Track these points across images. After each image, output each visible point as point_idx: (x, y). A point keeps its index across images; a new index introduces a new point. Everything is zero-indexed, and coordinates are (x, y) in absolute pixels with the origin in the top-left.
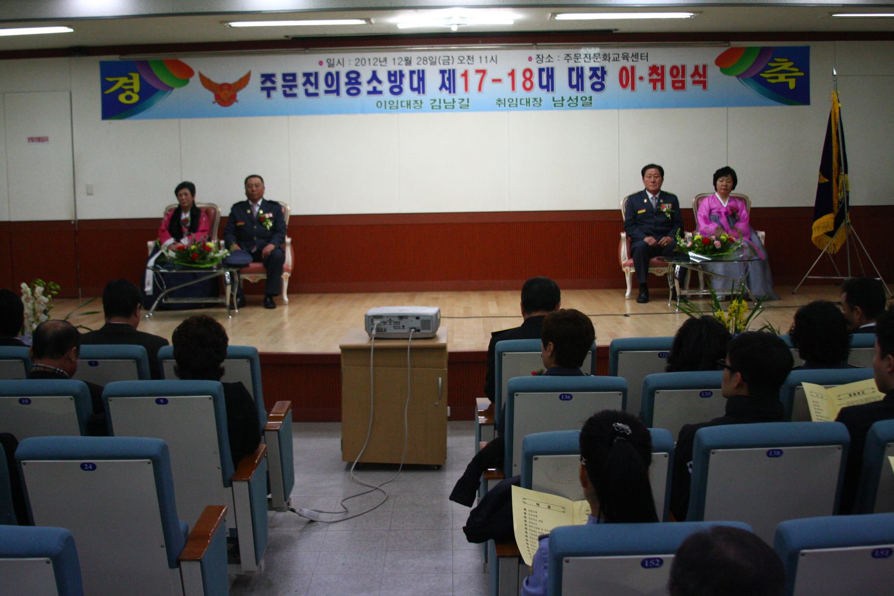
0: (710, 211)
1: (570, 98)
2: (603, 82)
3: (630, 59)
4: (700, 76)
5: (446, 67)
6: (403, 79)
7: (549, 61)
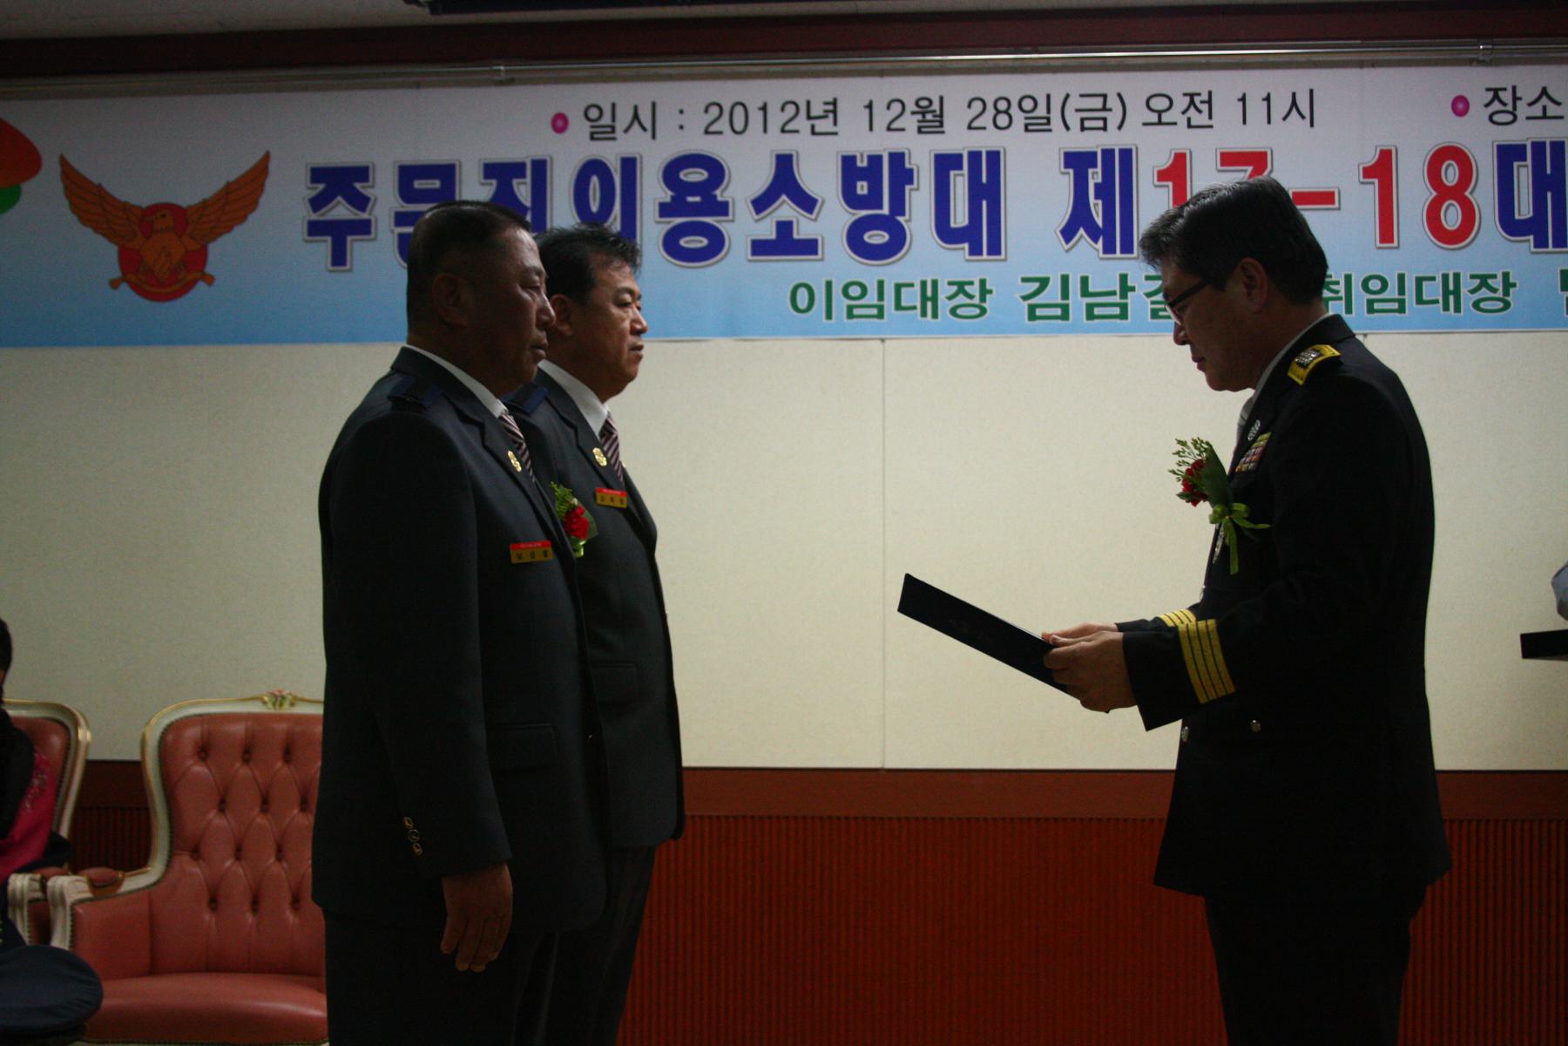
7: (1545, 116)
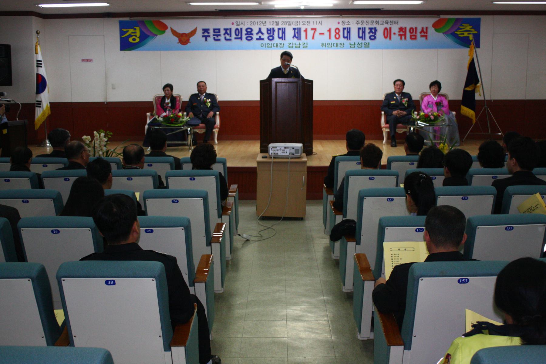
0: (428, 102)
1: (359, 43)
2: (375, 35)
3: (389, 24)
4: (424, 33)
5: (296, 27)
6: (274, 32)
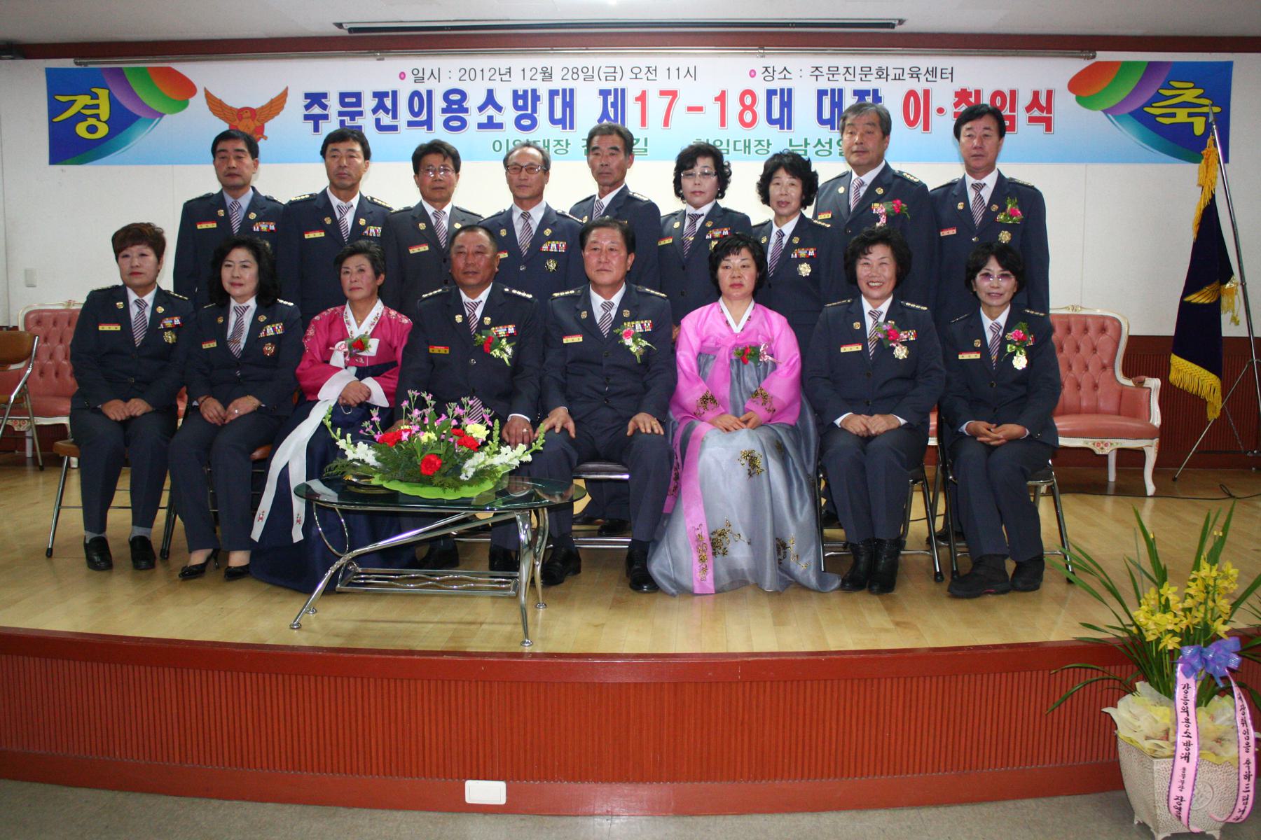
1: (819, 142)
5: (610, 86)
7: (785, 78)
